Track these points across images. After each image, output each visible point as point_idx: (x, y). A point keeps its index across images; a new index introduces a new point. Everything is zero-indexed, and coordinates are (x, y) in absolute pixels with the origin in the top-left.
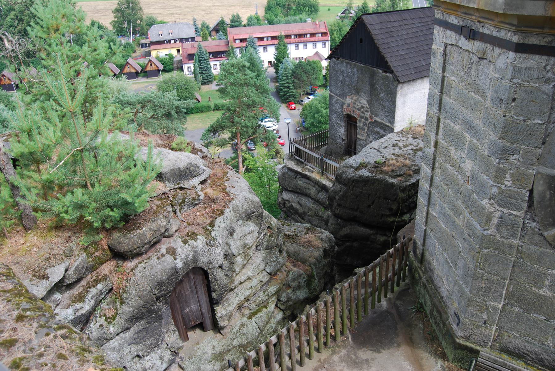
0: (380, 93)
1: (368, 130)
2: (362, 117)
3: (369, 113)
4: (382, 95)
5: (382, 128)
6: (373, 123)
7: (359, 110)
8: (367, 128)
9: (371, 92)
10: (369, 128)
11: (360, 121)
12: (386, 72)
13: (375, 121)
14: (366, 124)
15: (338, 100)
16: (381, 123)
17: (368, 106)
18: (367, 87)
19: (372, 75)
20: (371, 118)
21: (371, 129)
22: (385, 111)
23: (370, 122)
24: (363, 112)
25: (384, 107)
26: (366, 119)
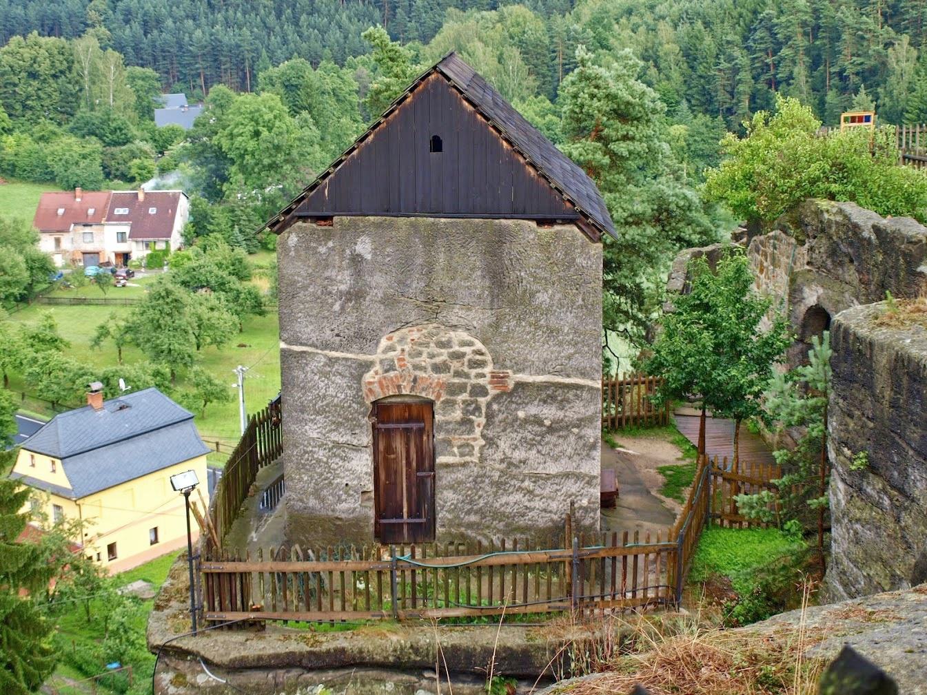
0: (532, 295)
1: (487, 426)
2: (454, 390)
3: (488, 370)
4: (543, 298)
5: (549, 400)
6: (511, 394)
7: (437, 368)
8: (483, 420)
9: (493, 297)
10: (490, 417)
11: (449, 404)
12: (551, 222)
13: (520, 385)
14: (478, 409)
15: (332, 361)
16: (547, 385)
17: (479, 345)
18: (479, 283)
19: (496, 246)
20: (498, 379)
21: (501, 417)
22: (560, 344)
23: (496, 398)
24: (458, 374)
25: (552, 332)
26: (480, 391)
